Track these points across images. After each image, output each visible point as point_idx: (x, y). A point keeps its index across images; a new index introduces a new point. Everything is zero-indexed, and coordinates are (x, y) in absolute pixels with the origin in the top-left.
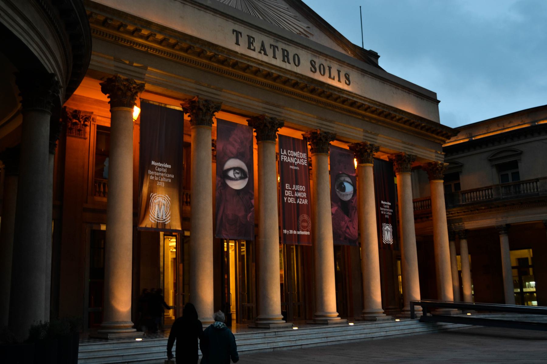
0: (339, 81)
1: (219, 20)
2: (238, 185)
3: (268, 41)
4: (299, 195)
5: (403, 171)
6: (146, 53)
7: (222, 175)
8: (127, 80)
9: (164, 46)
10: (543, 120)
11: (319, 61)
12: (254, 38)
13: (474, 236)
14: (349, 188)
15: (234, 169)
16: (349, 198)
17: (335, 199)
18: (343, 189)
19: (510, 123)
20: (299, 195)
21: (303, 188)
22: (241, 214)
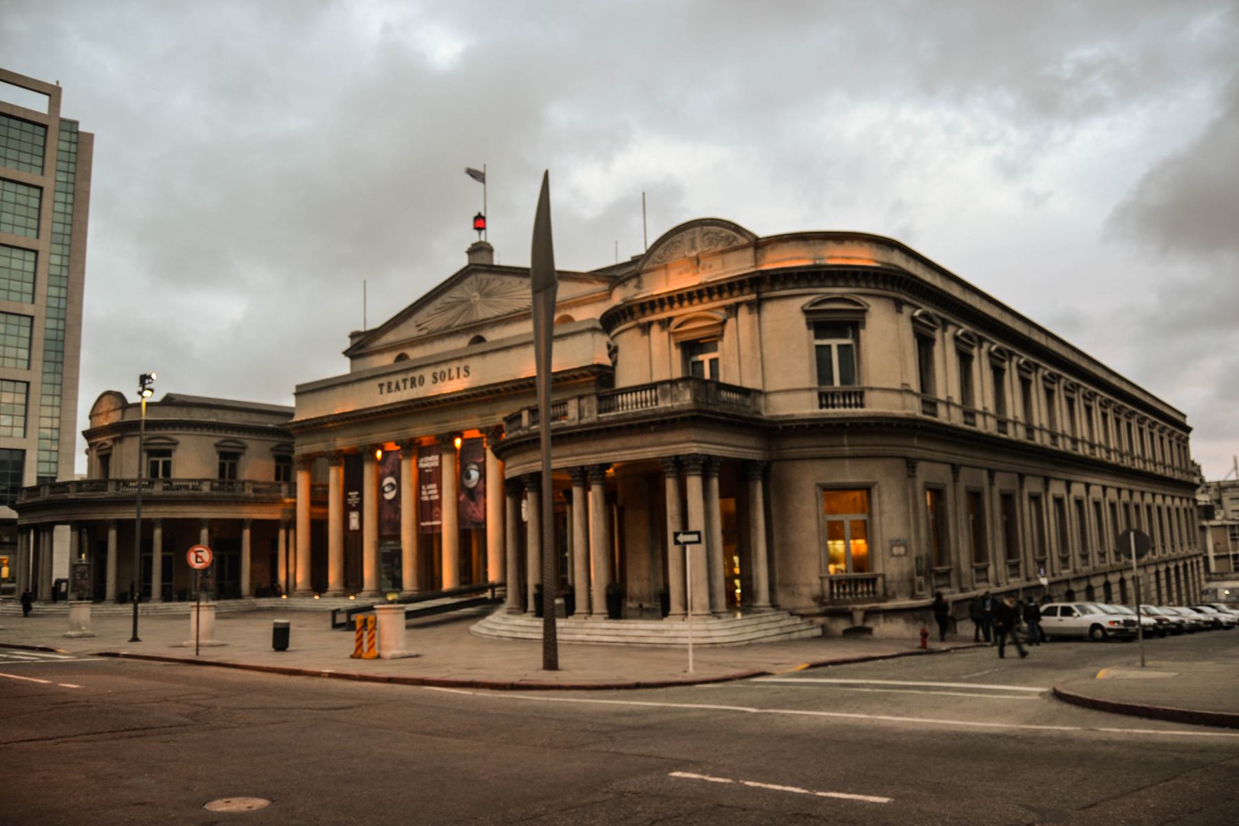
2: (389, 496)
3: (399, 378)
7: (380, 490)
11: (438, 370)
14: (475, 475)
18: (469, 477)
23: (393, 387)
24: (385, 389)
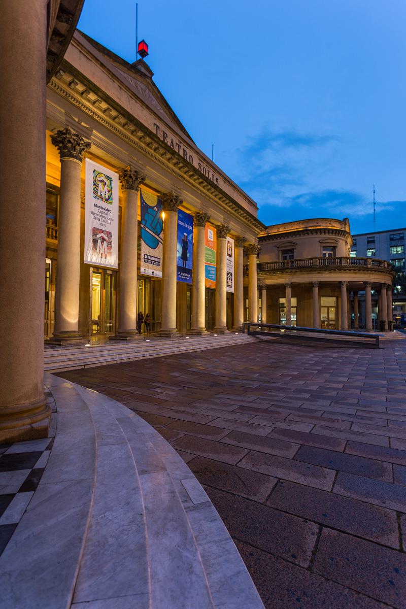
6: (91, 117)
8: (77, 136)
9: (107, 116)
10: (311, 227)
12: (167, 135)
13: (270, 288)
19: (292, 227)
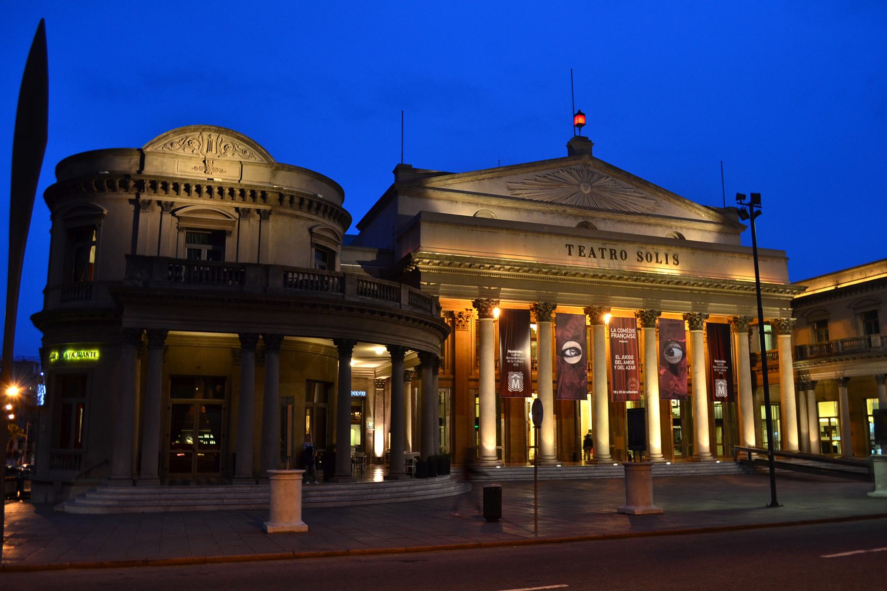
0: (667, 263)
1: (555, 240)
2: (575, 360)
3: (596, 246)
4: (628, 362)
5: (740, 330)
7: (560, 354)
14: (678, 353)
15: (570, 349)
16: (678, 361)
17: (663, 362)
18: (672, 354)
19: (872, 271)
20: (628, 362)
21: (632, 357)
22: (576, 382)
23: (587, 251)
24: (575, 251)
